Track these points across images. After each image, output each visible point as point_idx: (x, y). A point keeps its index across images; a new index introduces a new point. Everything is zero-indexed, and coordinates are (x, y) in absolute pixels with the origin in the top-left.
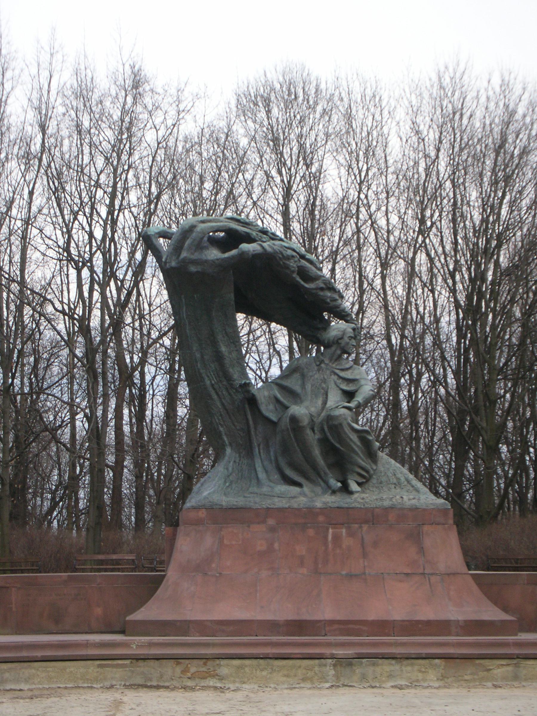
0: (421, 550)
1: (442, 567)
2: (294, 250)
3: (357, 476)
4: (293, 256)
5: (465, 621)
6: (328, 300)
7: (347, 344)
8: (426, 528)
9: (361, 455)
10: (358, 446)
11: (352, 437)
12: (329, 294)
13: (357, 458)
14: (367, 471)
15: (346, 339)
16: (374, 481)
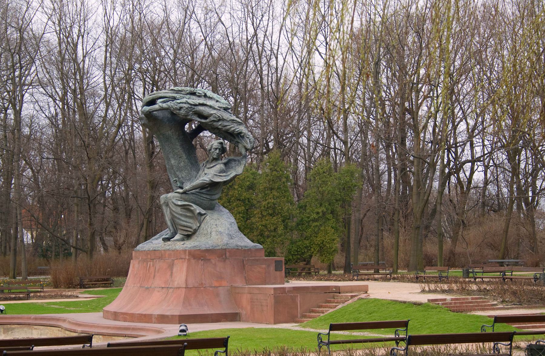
1: (176, 284)
2: (188, 103)
3: (182, 231)
4: (181, 108)
5: (158, 315)
6: (220, 127)
7: (213, 152)
8: (176, 261)
9: (183, 219)
10: (181, 215)
11: (174, 209)
13: (178, 221)
14: (191, 228)
15: (213, 150)
16: (197, 233)
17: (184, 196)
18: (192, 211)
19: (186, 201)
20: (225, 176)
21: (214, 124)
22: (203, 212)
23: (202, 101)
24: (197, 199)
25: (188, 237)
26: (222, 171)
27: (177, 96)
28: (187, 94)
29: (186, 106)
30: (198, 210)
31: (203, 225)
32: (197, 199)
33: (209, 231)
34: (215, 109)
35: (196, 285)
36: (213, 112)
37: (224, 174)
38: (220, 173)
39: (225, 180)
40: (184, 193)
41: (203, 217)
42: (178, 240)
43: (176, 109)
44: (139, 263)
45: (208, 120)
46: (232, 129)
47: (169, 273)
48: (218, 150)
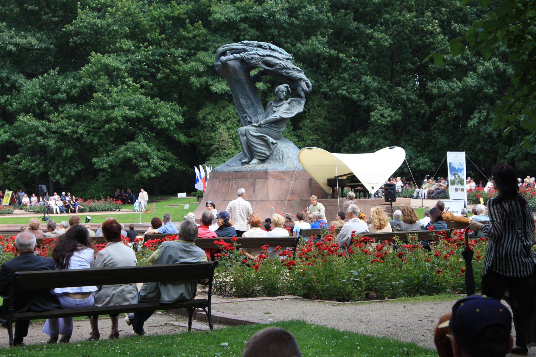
0: (254, 190)
4: (253, 58)
6: (284, 74)
8: (258, 180)
9: (258, 147)
10: (257, 144)
11: (251, 139)
12: (284, 71)
14: (265, 154)
16: (270, 158)
17: (258, 129)
18: (266, 142)
19: (261, 133)
20: (291, 113)
21: (279, 71)
22: (275, 141)
23: (268, 52)
24: (269, 131)
25: (263, 161)
26: (288, 109)
27: (247, 48)
28: (255, 46)
29: (257, 56)
30: (271, 140)
31: (275, 152)
32: (269, 131)
33: (281, 157)
34: (279, 59)
35: (275, 199)
36: (278, 61)
37: (289, 112)
38: (286, 111)
39: (291, 116)
40: (259, 126)
41: (275, 145)
42: (254, 164)
43: (248, 59)
44: (220, 181)
45: (274, 68)
46: (295, 75)
47: (252, 190)
48: (284, 93)
